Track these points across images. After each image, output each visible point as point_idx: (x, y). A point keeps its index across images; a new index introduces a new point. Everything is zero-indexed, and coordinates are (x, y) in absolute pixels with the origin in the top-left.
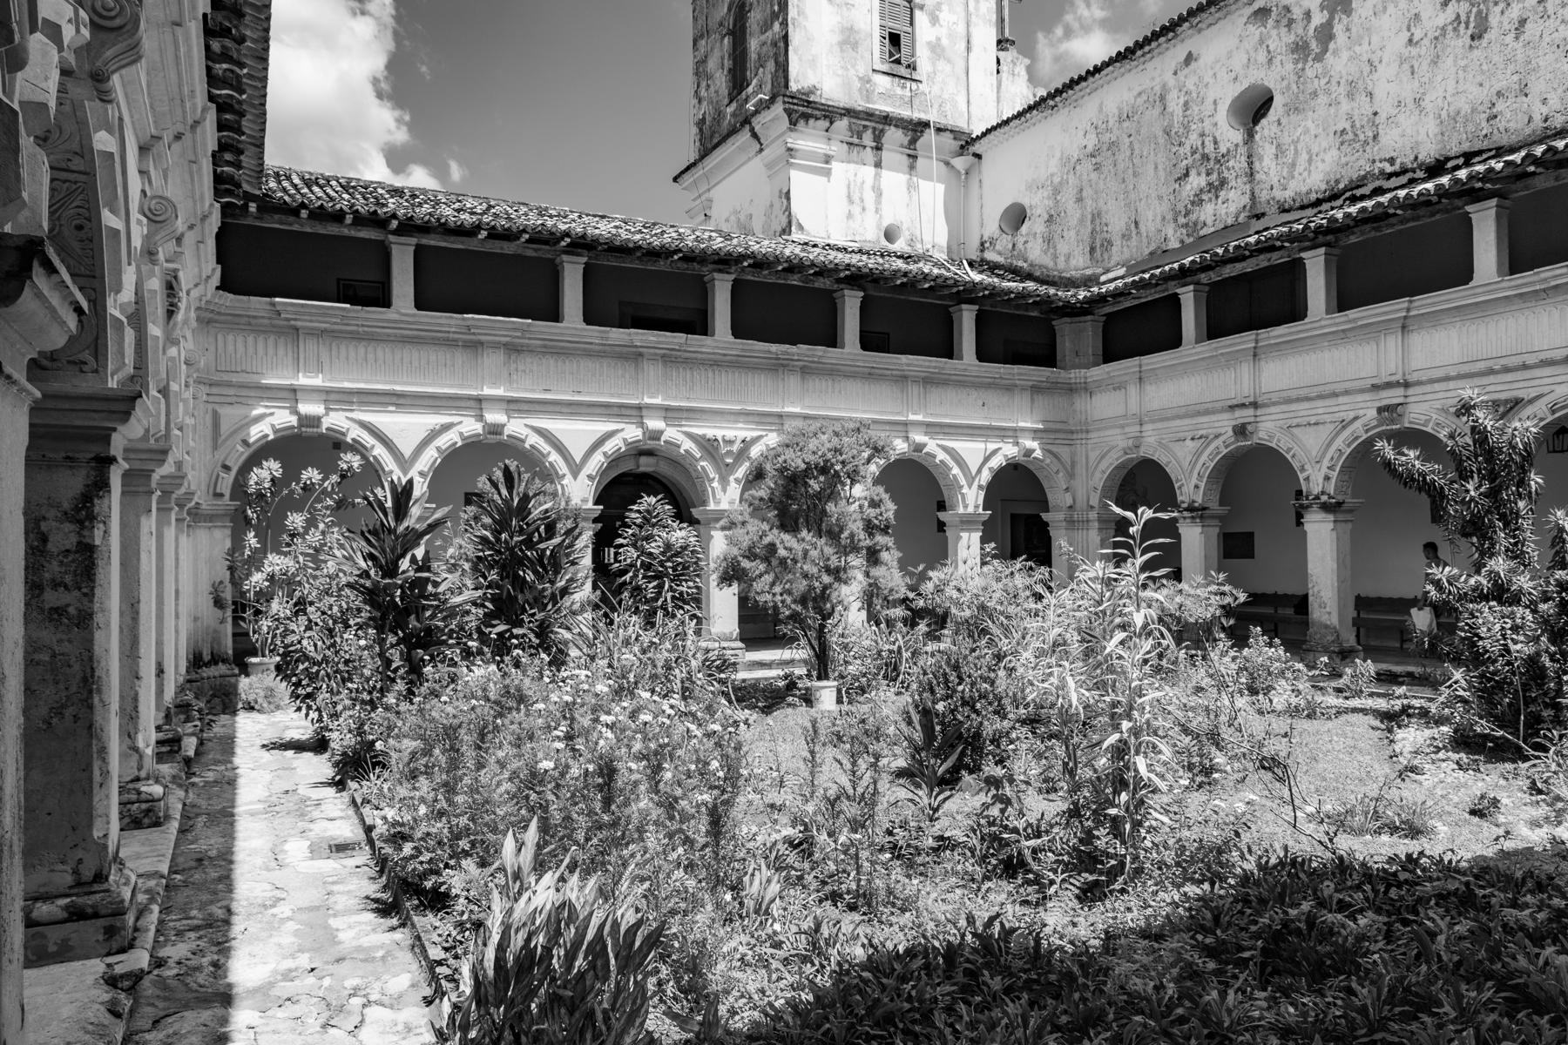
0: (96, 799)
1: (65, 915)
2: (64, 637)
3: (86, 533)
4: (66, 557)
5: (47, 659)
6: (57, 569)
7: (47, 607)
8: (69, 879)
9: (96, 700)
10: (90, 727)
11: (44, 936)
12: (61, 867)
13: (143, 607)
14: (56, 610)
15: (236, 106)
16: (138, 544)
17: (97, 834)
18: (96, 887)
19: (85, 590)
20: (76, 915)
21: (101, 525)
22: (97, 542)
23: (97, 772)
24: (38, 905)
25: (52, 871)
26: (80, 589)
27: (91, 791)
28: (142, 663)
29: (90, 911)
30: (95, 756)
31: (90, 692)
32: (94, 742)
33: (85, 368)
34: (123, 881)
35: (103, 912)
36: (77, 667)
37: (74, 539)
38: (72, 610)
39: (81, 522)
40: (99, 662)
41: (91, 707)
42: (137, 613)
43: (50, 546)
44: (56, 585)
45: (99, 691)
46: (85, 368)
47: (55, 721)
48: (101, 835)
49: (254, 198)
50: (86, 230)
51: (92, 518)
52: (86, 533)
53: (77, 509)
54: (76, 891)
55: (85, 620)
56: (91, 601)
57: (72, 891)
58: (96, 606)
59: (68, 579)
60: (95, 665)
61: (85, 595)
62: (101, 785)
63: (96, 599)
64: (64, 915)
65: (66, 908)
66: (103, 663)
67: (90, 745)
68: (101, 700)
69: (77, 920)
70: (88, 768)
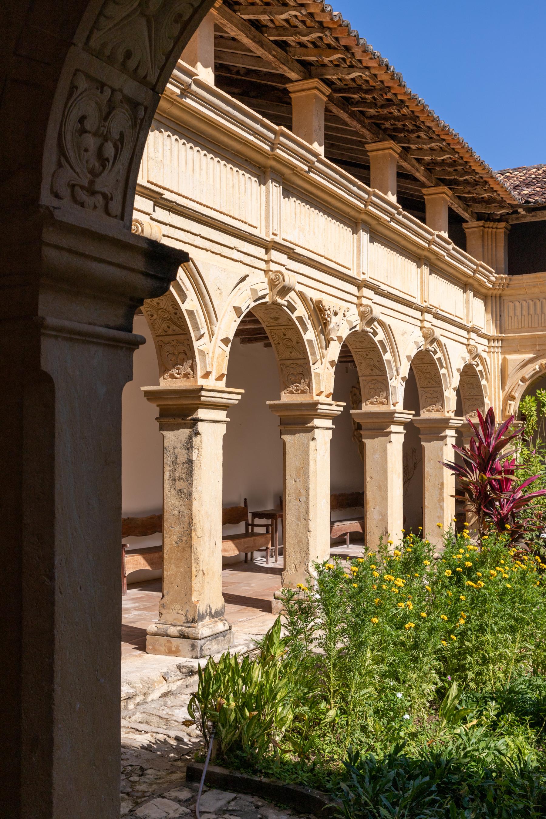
0: (193, 582)
1: (179, 635)
2: (183, 503)
3: (190, 454)
4: (183, 466)
5: (177, 513)
6: (181, 471)
7: (177, 488)
8: (184, 619)
9: (193, 534)
10: (191, 547)
11: (171, 643)
12: (180, 612)
13: (311, 491)
14: (180, 490)
15: (460, 161)
16: (309, 457)
17: (194, 599)
18: (193, 625)
19: (189, 482)
20: (183, 636)
21: (196, 451)
22: (194, 459)
23: (194, 570)
24: (172, 628)
25: (178, 613)
26: (188, 481)
27: (191, 578)
28: (311, 523)
29: (186, 634)
30: (193, 561)
31: (191, 530)
32: (193, 555)
33: (190, 376)
34: (211, 626)
35: (191, 636)
36: (187, 518)
37: (186, 457)
38: (185, 490)
39: (188, 449)
40: (195, 516)
41: (191, 537)
42: (309, 495)
43: (178, 459)
44: (180, 479)
45: (195, 530)
46: (190, 376)
47: (179, 542)
48: (196, 600)
49: (520, 206)
50: (178, 314)
51: (192, 447)
52: (190, 454)
53: (187, 443)
54: (185, 625)
55: (189, 495)
56: (192, 487)
57: (185, 625)
58: (194, 489)
59: (184, 476)
60: (193, 518)
61: (190, 484)
62: (196, 576)
63: (193, 486)
64: (177, 634)
65: (179, 631)
66: (197, 517)
67: (191, 556)
68: (196, 535)
69: (183, 638)
70: (190, 567)
